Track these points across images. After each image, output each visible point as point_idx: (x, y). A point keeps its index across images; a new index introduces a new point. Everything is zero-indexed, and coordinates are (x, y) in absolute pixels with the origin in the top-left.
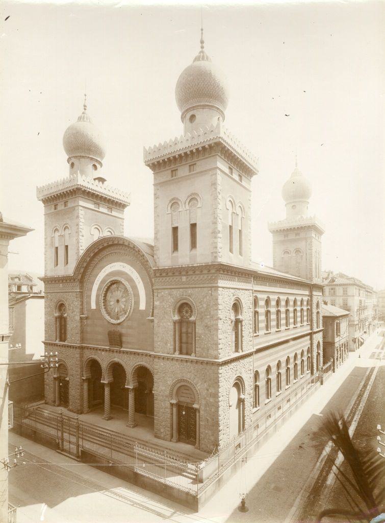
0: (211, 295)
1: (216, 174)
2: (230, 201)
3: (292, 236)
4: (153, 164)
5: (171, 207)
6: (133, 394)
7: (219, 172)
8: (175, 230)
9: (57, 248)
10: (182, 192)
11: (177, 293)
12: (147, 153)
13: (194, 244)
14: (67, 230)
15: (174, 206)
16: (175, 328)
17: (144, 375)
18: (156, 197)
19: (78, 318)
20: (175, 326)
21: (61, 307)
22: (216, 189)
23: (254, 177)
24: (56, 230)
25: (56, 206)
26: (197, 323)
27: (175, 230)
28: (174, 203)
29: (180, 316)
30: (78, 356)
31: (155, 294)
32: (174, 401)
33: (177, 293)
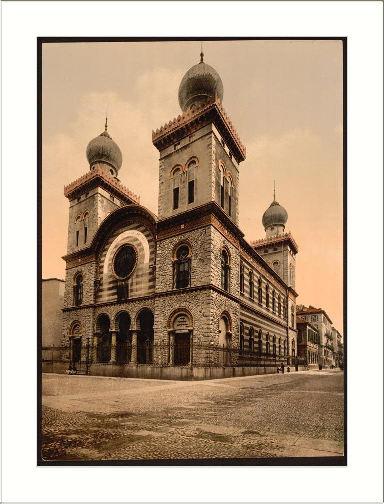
0: (205, 233)
1: (211, 137)
2: (221, 166)
3: (270, 251)
4: (160, 142)
5: (173, 175)
6: (136, 336)
7: (213, 136)
8: (176, 191)
9: (78, 232)
10: (182, 159)
11: (176, 240)
12: (154, 135)
13: (191, 200)
14: (87, 216)
15: (177, 173)
16: (174, 270)
17: (147, 318)
18: (161, 170)
19: (92, 283)
20: (174, 267)
21: (79, 278)
22: (211, 149)
23: (241, 163)
24: (79, 218)
25: (79, 199)
26: (193, 258)
27: (176, 191)
28: (176, 169)
29: (178, 257)
30: (92, 314)
31: (158, 246)
32: (172, 330)
33: (176, 240)
